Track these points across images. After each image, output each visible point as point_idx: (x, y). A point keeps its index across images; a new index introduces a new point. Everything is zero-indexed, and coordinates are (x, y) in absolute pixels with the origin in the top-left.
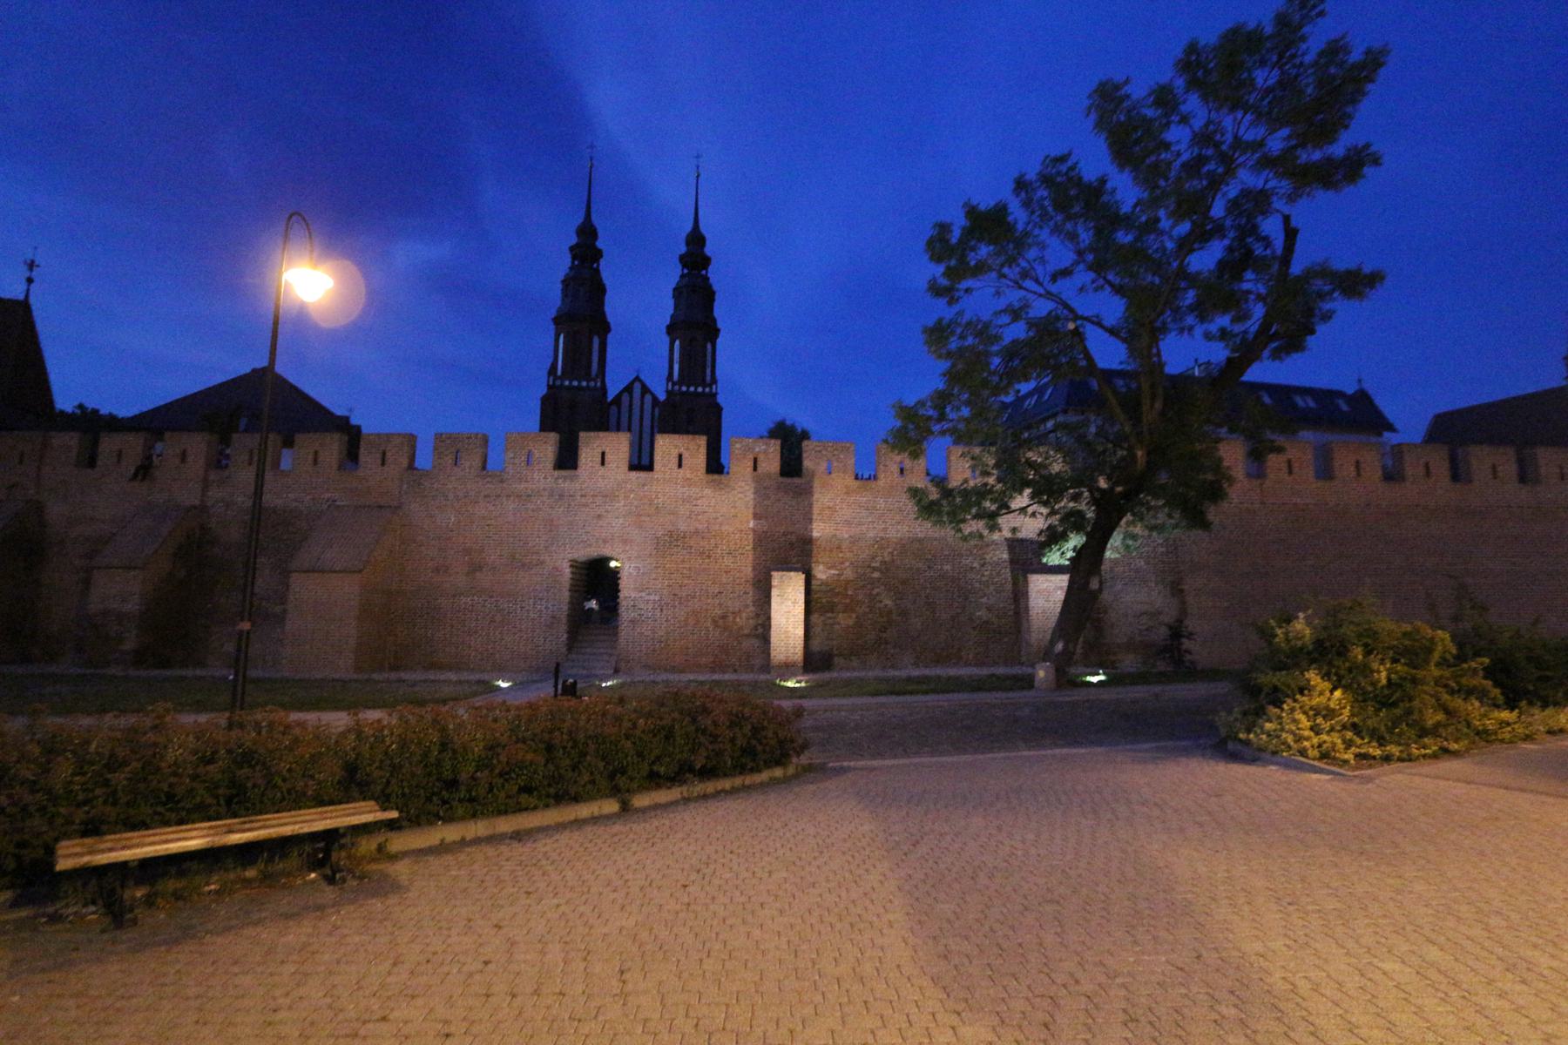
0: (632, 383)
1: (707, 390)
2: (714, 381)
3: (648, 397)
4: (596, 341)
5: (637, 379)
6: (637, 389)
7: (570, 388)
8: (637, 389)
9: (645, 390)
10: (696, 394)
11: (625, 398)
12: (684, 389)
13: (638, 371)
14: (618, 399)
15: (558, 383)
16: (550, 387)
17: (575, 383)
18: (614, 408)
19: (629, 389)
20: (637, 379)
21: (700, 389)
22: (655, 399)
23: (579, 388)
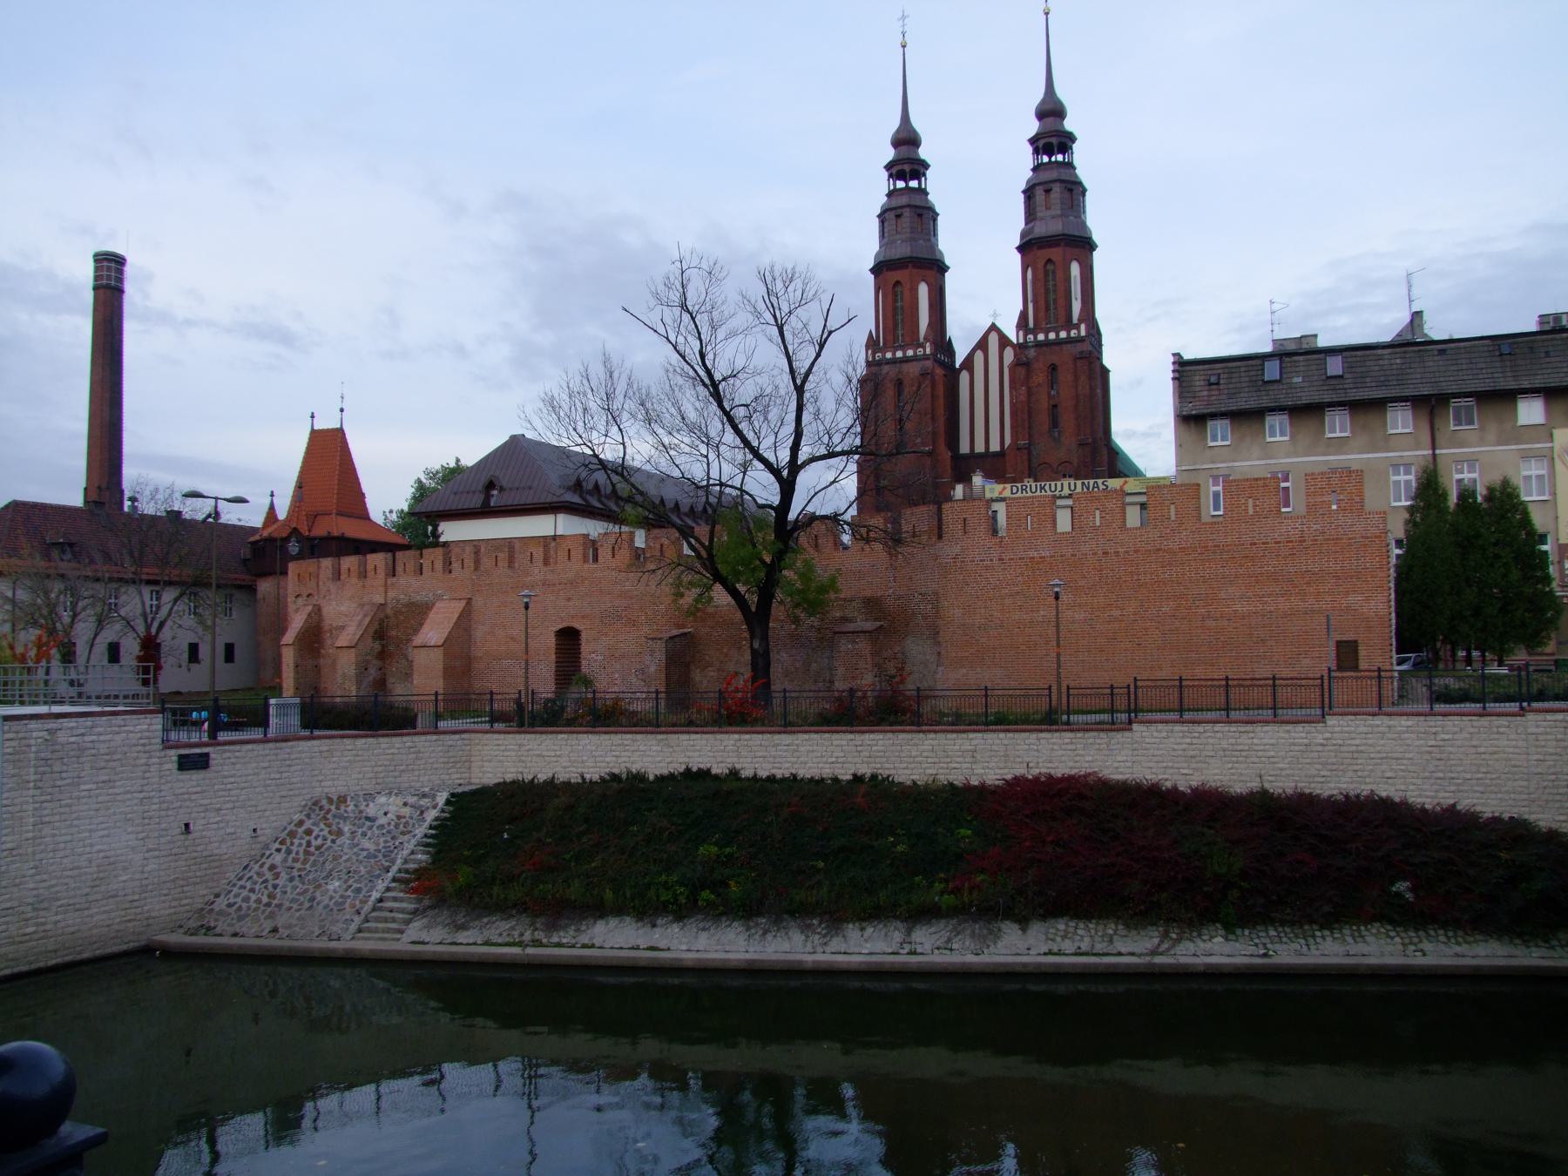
1: (1073, 333)
4: (923, 290)
5: (993, 328)
6: (993, 340)
7: (894, 361)
8: (993, 340)
11: (979, 355)
12: (1041, 337)
13: (995, 315)
14: (968, 363)
16: (869, 364)
17: (899, 354)
18: (964, 376)
19: (982, 345)
20: (993, 328)
21: (1063, 334)
23: (905, 360)
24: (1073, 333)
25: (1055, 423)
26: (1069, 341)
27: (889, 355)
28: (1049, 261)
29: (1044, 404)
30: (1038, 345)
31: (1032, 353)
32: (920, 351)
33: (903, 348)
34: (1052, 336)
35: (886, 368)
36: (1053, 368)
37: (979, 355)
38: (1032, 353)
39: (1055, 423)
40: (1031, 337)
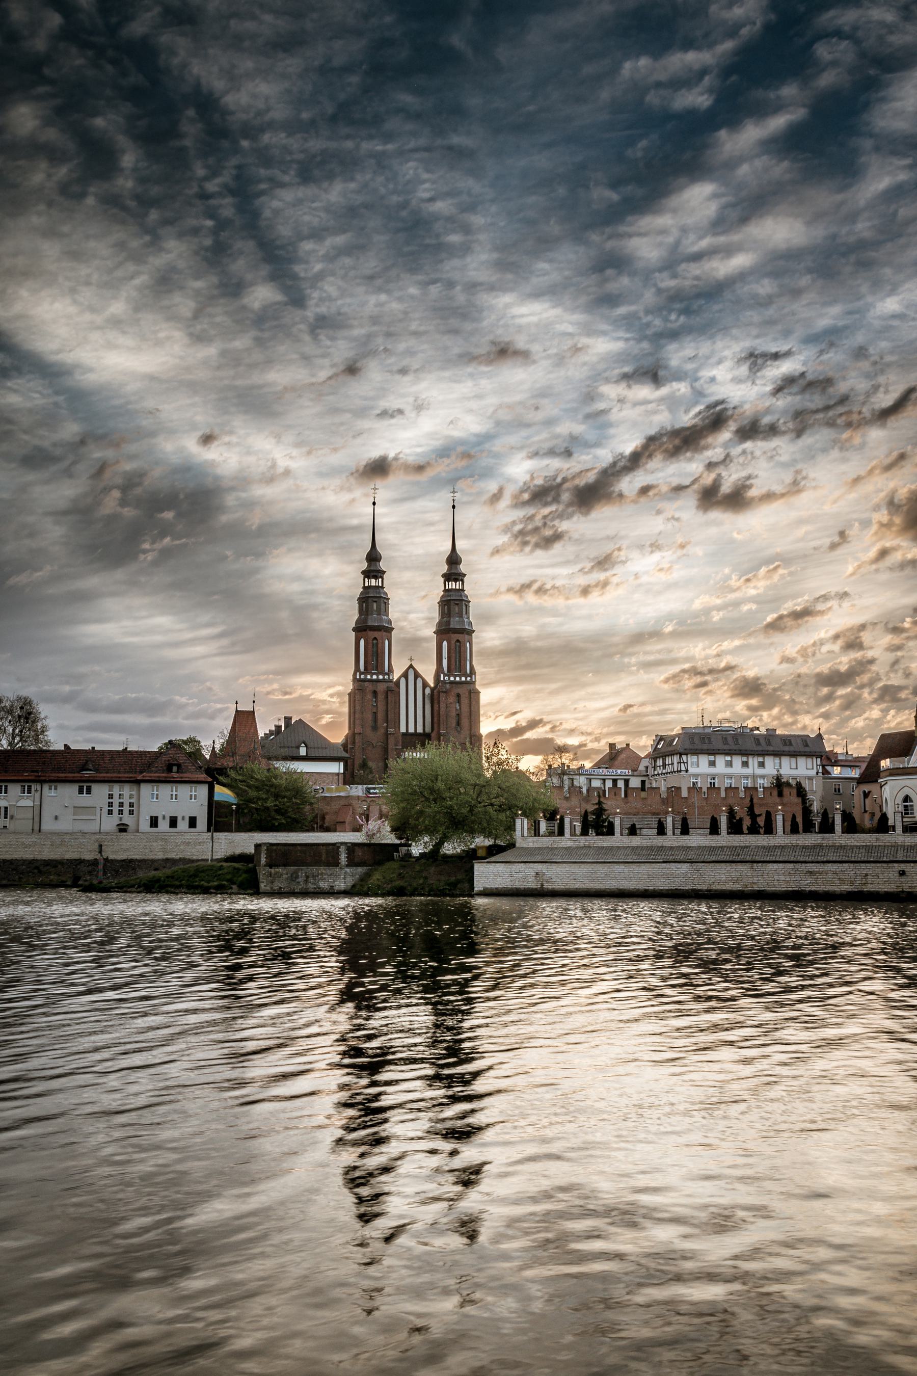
0: (407, 671)
1: (469, 679)
2: (472, 671)
3: (419, 681)
4: (387, 642)
5: (411, 666)
7: (371, 681)
9: (417, 675)
10: (461, 683)
11: (403, 681)
12: (452, 679)
15: (363, 676)
17: (375, 677)
20: (411, 666)
21: (463, 679)
22: (425, 685)
23: (378, 681)
24: (469, 679)
25: (458, 724)
26: (466, 683)
27: (369, 677)
28: (458, 641)
29: (453, 714)
30: (451, 683)
31: (448, 686)
32: (386, 677)
33: (377, 675)
34: (458, 679)
35: (366, 684)
36: (458, 695)
37: (403, 681)
38: (448, 686)
39: (458, 724)
40: (446, 678)
